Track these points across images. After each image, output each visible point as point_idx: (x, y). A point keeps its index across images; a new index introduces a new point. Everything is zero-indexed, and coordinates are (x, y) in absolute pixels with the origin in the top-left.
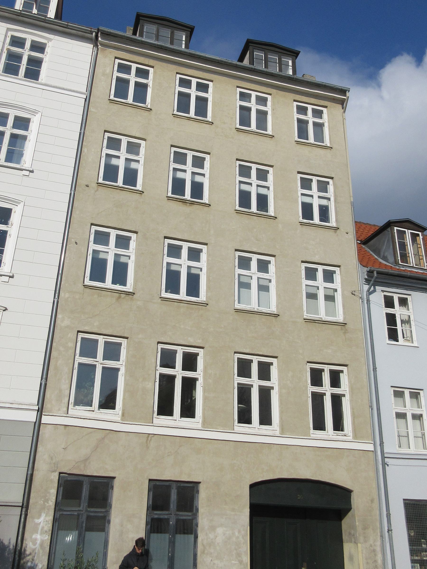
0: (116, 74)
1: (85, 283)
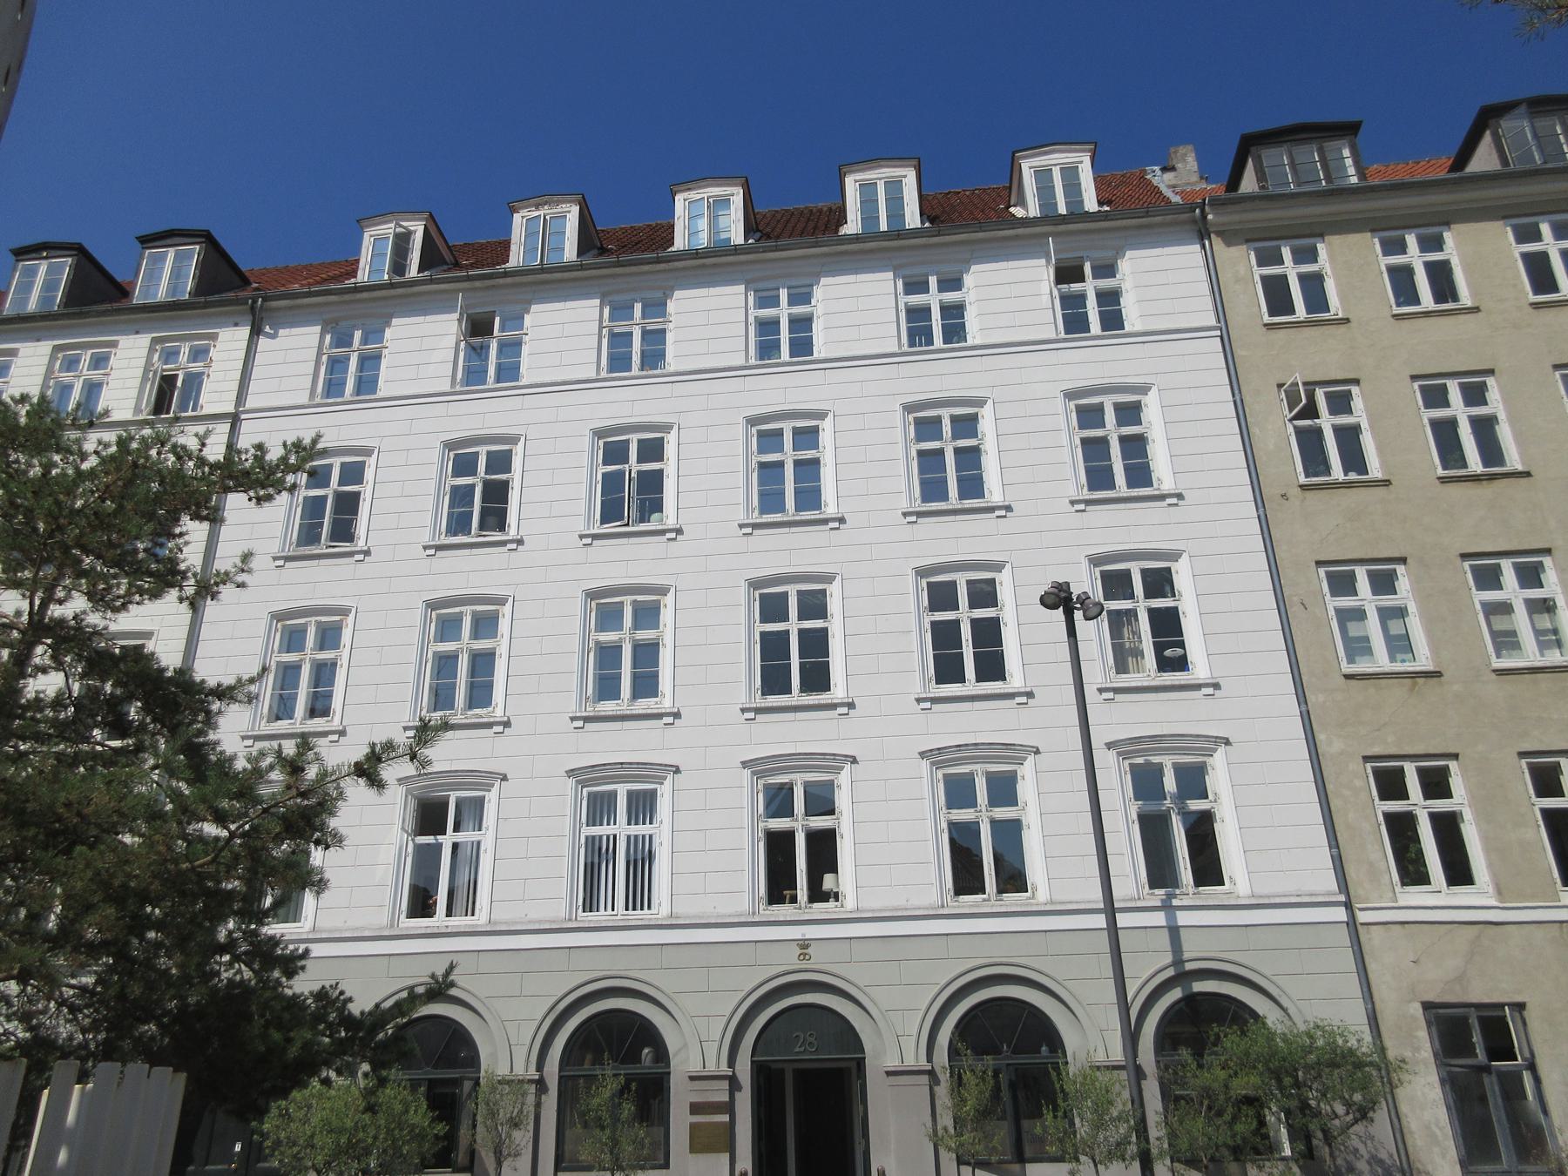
0: (1258, 272)
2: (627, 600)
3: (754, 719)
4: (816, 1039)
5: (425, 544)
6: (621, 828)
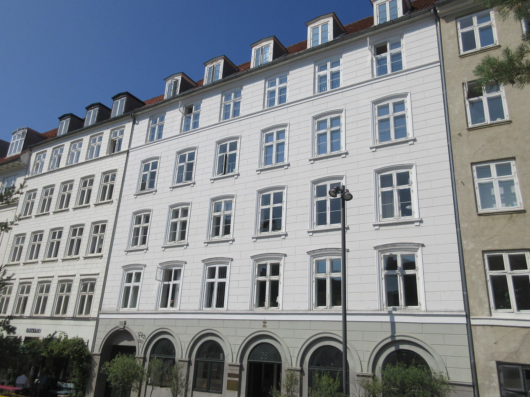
1: (479, 212)
3: (256, 241)
4: (267, 355)
5: (170, 187)
6: (217, 280)
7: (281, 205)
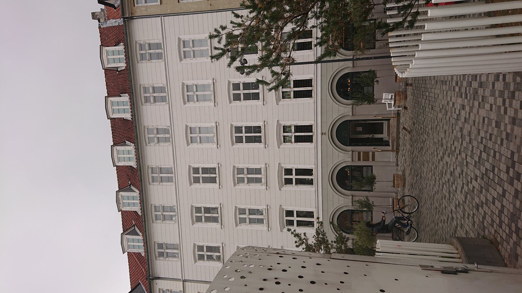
2: (236, 176)
7: (244, 127)
